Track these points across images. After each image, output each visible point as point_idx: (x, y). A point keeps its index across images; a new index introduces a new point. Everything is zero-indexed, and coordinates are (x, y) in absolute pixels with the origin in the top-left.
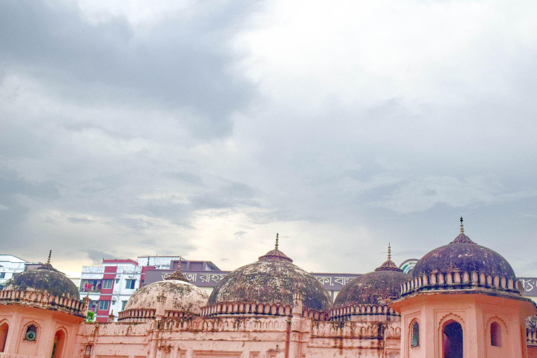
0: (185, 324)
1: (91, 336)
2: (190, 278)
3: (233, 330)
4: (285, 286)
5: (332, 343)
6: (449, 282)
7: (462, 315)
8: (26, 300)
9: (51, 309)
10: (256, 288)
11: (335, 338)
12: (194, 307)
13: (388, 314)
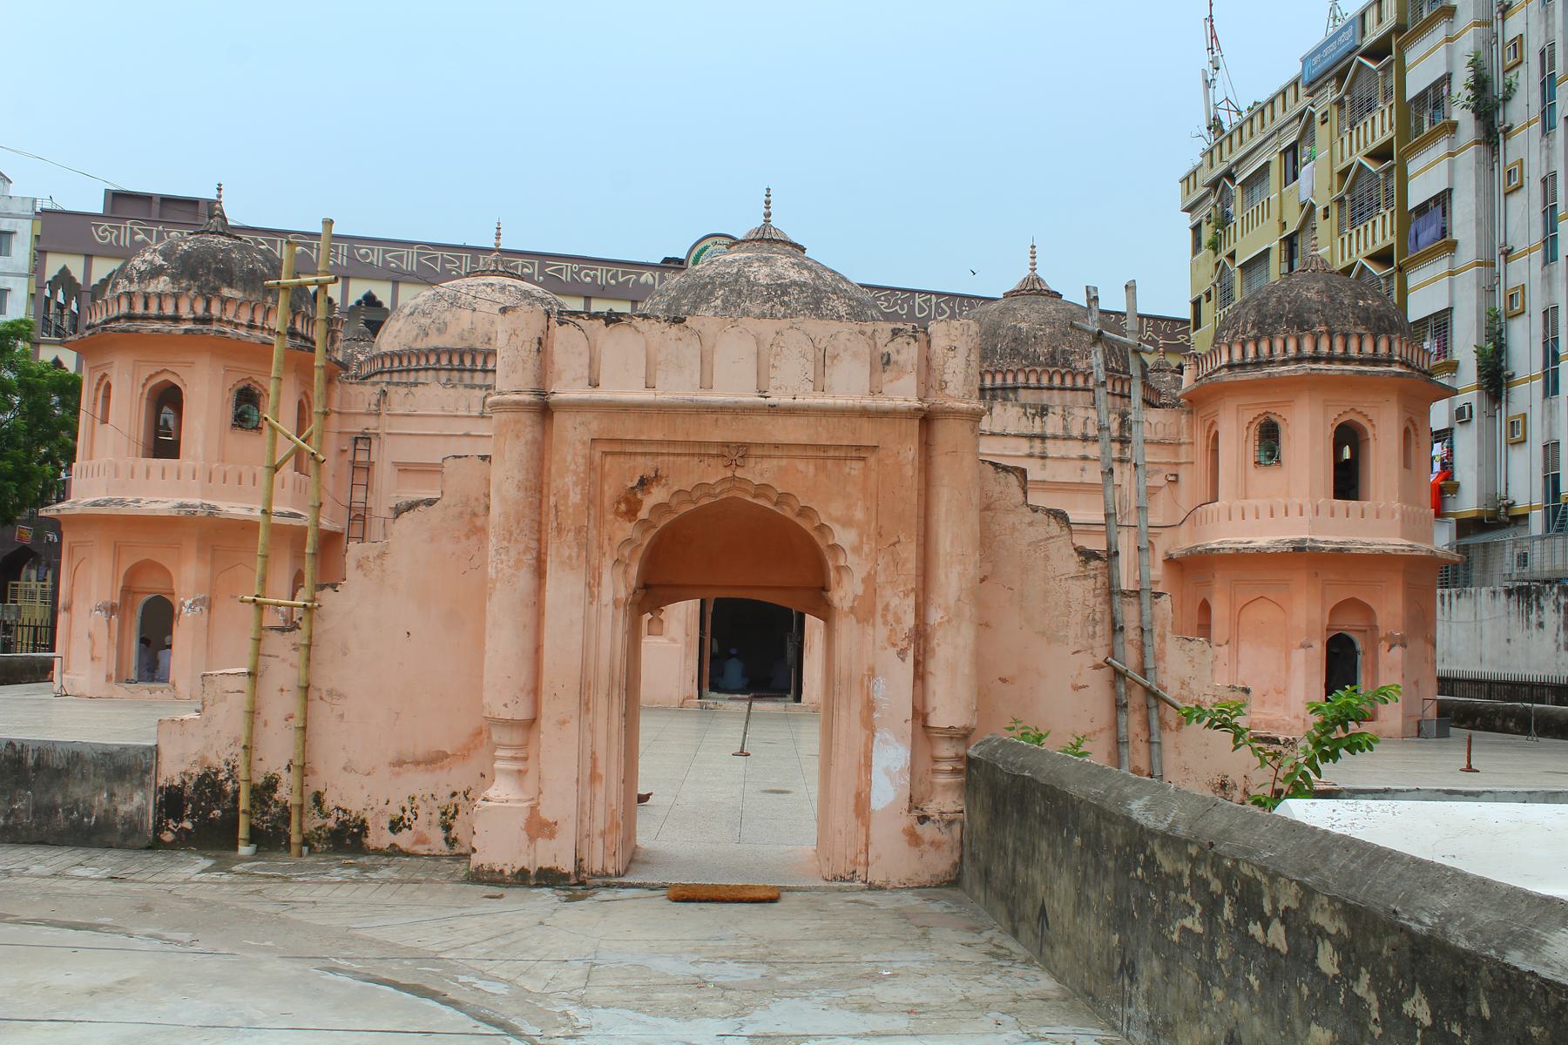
1: (369, 414)
6: (1353, 350)
7: (1371, 413)
8: (229, 322)
9: (300, 348)
11: (1031, 437)
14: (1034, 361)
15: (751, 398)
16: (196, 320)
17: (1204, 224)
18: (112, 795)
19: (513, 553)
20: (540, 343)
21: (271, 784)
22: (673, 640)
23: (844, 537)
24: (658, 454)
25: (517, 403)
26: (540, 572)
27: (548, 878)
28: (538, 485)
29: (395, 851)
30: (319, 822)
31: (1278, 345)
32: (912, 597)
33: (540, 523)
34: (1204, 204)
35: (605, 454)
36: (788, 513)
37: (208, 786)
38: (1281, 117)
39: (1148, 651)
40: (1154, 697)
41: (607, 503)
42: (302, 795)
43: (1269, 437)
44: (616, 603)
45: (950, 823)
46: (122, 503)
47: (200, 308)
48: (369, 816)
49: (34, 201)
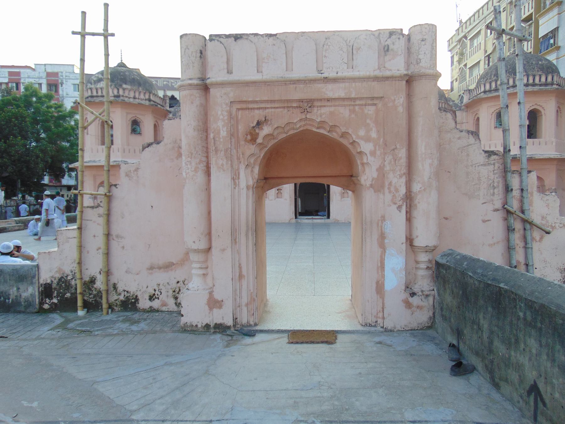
8: (126, 97)
9: (152, 105)
15: (313, 74)
17: (455, 56)
18: (18, 289)
19: (193, 164)
20: (201, 53)
21: (93, 281)
22: (286, 199)
23: (366, 147)
24: (266, 108)
25: (190, 85)
26: (208, 173)
27: (220, 328)
29: (152, 310)
30: (116, 297)
32: (404, 177)
33: (207, 148)
34: (455, 48)
35: (238, 109)
36: (334, 135)
37: (63, 282)
38: (486, 13)
39: (525, 201)
42: (107, 285)
44: (248, 187)
45: (427, 296)
46: (94, 161)
48: (139, 294)
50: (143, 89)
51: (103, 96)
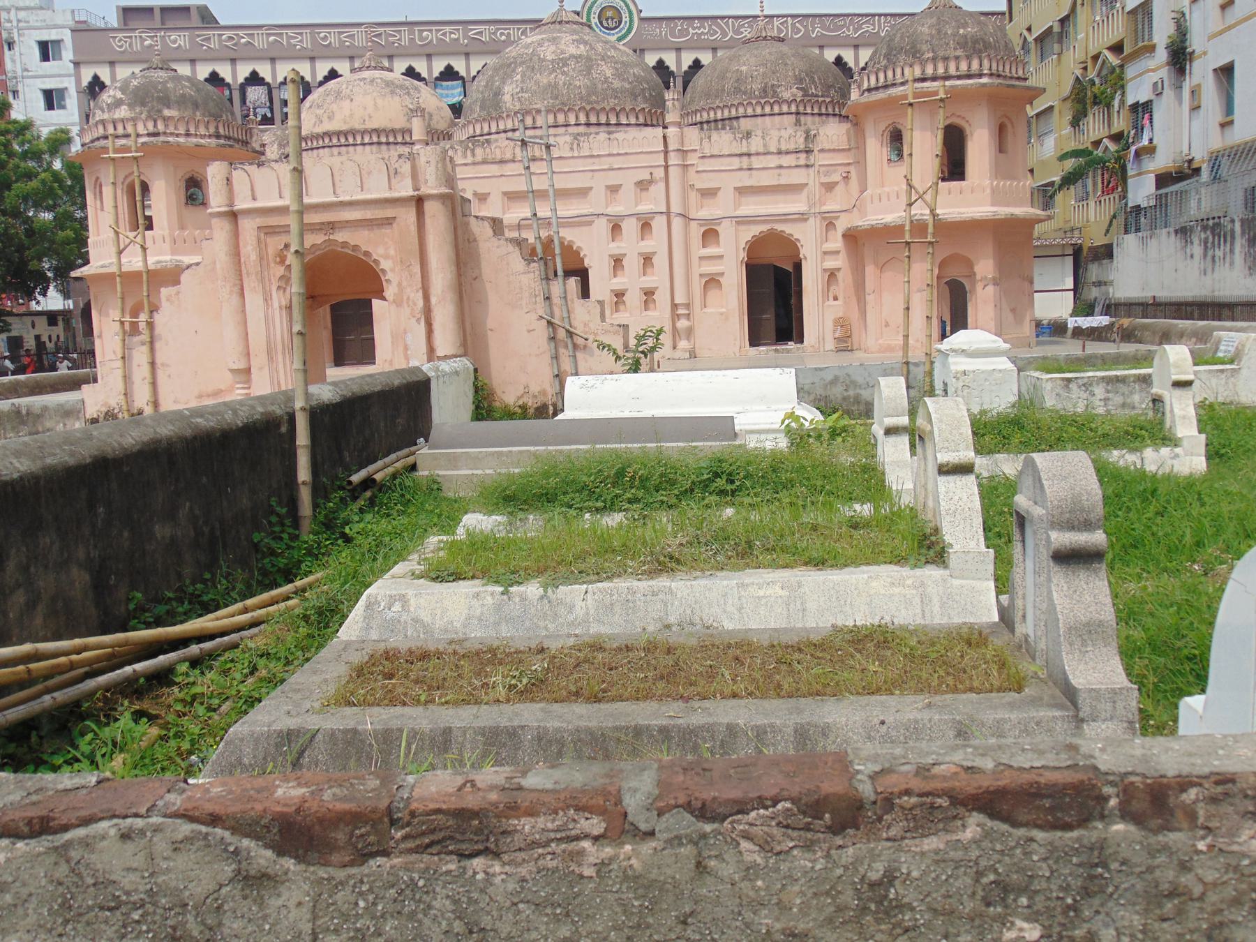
0: (479, 151)
2: (175, 42)
3: (570, 155)
4: (618, 75)
5: (736, 163)
6: (952, 71)
8: (172, 134)
9: (224, 146)
10: (578, 83)
11: (741, 155)
12: (435, 117)
13: (798, 113)
14: (751, 94)
15: (332, 199)
16: (149, 135)
23: (385, 264)
28: (236, 253)
31: (899, 71)
40: (570, 334)
41: (270, 258)
43: (896, 138)
47: (150, 125)
49: (73, 12)
50: (203, 115)
51: (127, 136)
